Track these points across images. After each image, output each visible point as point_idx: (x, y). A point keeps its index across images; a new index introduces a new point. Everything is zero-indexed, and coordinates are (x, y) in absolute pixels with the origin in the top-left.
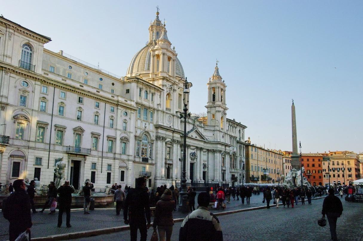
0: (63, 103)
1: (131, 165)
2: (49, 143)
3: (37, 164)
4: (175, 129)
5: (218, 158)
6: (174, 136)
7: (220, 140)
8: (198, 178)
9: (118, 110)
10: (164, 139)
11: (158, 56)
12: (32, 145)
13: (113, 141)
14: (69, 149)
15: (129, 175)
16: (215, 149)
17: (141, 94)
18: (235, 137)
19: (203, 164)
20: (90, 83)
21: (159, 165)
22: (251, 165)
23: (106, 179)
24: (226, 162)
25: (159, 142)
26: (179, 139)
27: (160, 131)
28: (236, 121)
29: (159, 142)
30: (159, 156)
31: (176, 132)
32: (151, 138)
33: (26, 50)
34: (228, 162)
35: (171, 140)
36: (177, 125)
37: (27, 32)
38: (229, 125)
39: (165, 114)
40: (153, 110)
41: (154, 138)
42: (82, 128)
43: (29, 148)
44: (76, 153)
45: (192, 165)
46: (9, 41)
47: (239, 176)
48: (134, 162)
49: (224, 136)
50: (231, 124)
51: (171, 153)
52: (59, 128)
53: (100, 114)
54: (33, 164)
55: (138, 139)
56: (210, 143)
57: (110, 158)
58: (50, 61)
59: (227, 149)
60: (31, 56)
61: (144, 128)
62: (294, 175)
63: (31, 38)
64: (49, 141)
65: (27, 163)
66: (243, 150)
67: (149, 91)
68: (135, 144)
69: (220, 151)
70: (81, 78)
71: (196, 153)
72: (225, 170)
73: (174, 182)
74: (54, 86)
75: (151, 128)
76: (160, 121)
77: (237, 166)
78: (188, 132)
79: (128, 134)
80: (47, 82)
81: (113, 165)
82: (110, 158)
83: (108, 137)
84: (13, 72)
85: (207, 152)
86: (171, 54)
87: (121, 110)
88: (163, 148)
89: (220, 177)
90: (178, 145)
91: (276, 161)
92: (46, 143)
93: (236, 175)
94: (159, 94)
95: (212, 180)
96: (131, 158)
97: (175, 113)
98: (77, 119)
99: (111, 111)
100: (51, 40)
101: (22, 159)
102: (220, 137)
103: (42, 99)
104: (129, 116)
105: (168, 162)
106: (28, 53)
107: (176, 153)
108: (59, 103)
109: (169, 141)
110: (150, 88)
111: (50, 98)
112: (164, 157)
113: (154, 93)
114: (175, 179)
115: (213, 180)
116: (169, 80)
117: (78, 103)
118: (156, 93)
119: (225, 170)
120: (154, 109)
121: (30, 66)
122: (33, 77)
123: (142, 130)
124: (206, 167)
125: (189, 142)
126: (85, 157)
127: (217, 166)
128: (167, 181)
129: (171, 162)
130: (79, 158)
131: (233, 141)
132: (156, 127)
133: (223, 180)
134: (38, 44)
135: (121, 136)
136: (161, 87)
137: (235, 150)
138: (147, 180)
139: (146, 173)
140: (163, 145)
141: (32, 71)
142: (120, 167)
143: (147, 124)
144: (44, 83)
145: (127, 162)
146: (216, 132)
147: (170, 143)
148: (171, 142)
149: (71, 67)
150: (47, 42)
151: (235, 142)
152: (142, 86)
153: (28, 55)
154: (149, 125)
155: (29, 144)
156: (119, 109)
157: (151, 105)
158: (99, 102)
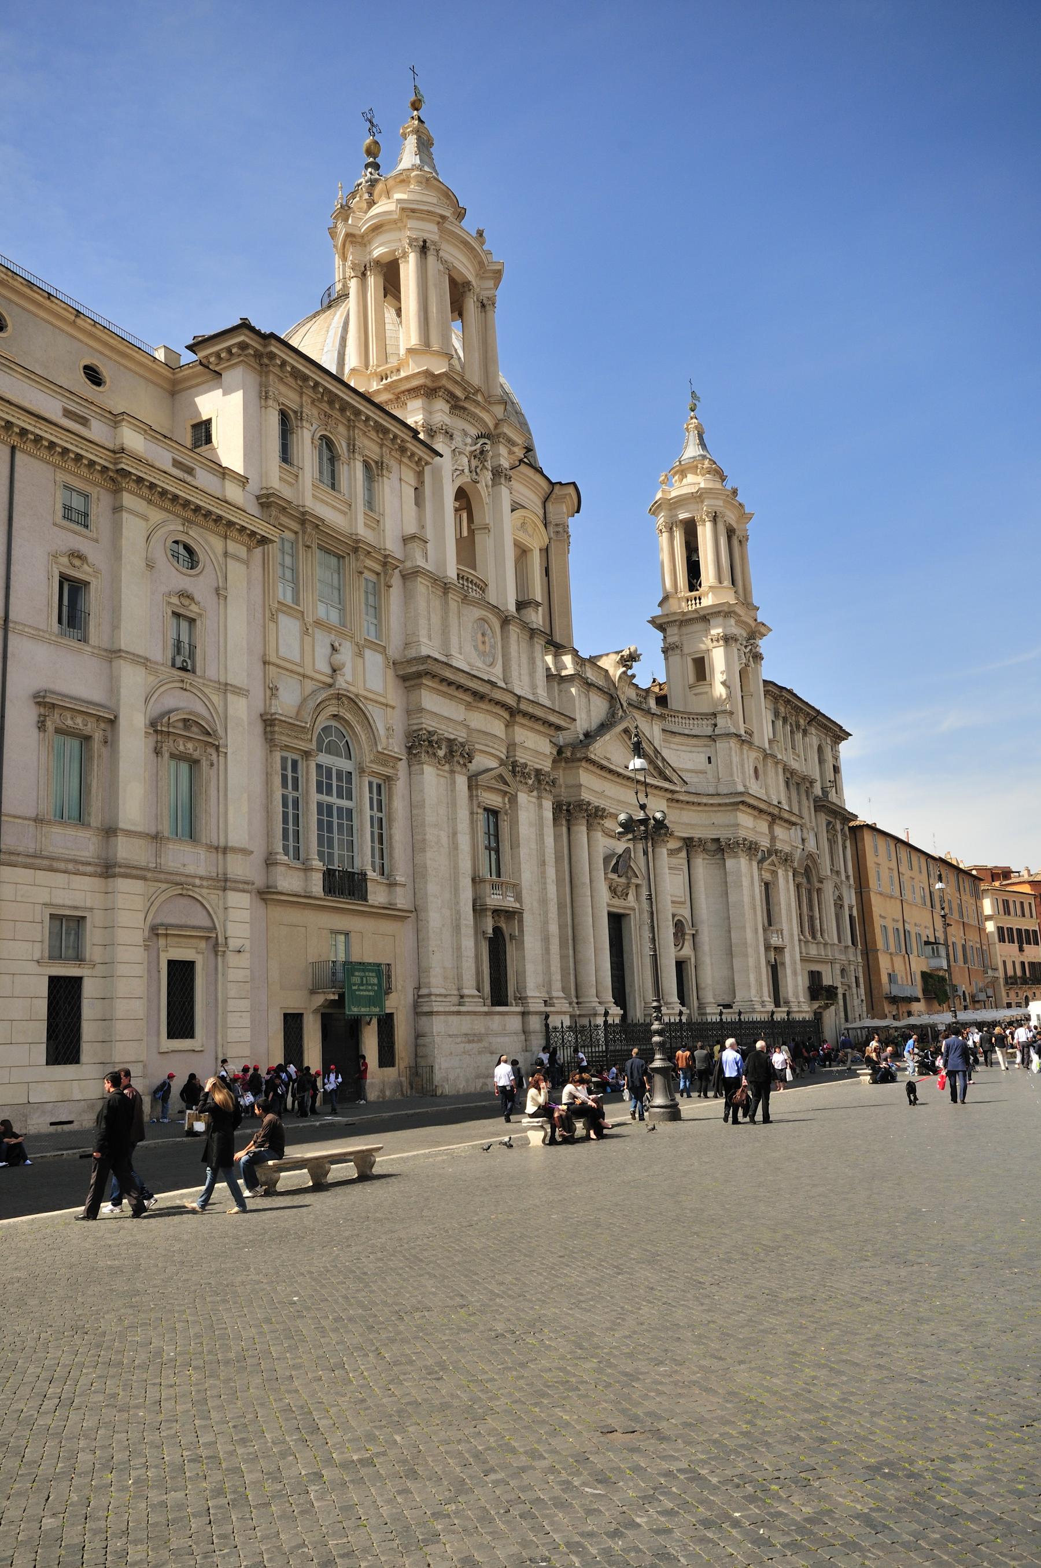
1: (246, 915)
5: (746, 882)
7: (745, 786)
9: (125, 515)
13: (87, 739)
15: (232, 993)
16: (723, 834)
18: (804, 778)
21: (436, 918)
22: (878, 923)
23: (40, 1030)
25: (425, 766)
26: (546, 765)
29: (425, 766)
30: (436, 860)
31: (525, 714)
32: (374, 740)
34: (789, 905)
35: (502, 763)
36: (526, 679)
38: (776, 714)
39: (453, 605)
40: (378, 568)
41: (396, 746)
47: (839, 978)
48: (266, 895)
49: (760, 772)
50: (782, 709)
55: (285, 740)
57: (74, 867)
59: (780, 837)
61: (329, 671)
66: (844, 848)
67: (344, 445)
68: (268, 776)
69: (750, 849)
72: (779, 950)
73: (535, 1023)
76: (430, 639)
78: (587, 735)
79: (215, 698)
82: (70, 867)
85: (684, 854)
86: (465, 261)
87: (146, 519)
88: (455, 812)
89: (760, 985)
90: (539, 798)
94: (410, 477)
96: (238, 868)
97: (512, 607)
102: (743, 773)
104: (209, 569)
105: (494, 900)
107: (533, 846)
110: (350, 426)
112: (466, 866)
113: (380, 465)
114: (543, 1008)
115: (728, 1006)
116: (466, 405)
118: (393, 463)
119: (779, 950)
120: (386, 562)
123: (310, 686)
124: (683, 934)
128: (497, 1017)
129: (509, 902)
132: (404, 678)
133: (777, 1004)
135: (155, 709)
138: (369, 1023)
140: (453, 790)
142: (155, 931)
145: (212, 898)
146: (721, 745)
147: (494, 784)
148: (501, 778)
151: (809, 807)
152: (294, 396)
154: (360, 654)
156: (131, 512)
157: (362, 531)
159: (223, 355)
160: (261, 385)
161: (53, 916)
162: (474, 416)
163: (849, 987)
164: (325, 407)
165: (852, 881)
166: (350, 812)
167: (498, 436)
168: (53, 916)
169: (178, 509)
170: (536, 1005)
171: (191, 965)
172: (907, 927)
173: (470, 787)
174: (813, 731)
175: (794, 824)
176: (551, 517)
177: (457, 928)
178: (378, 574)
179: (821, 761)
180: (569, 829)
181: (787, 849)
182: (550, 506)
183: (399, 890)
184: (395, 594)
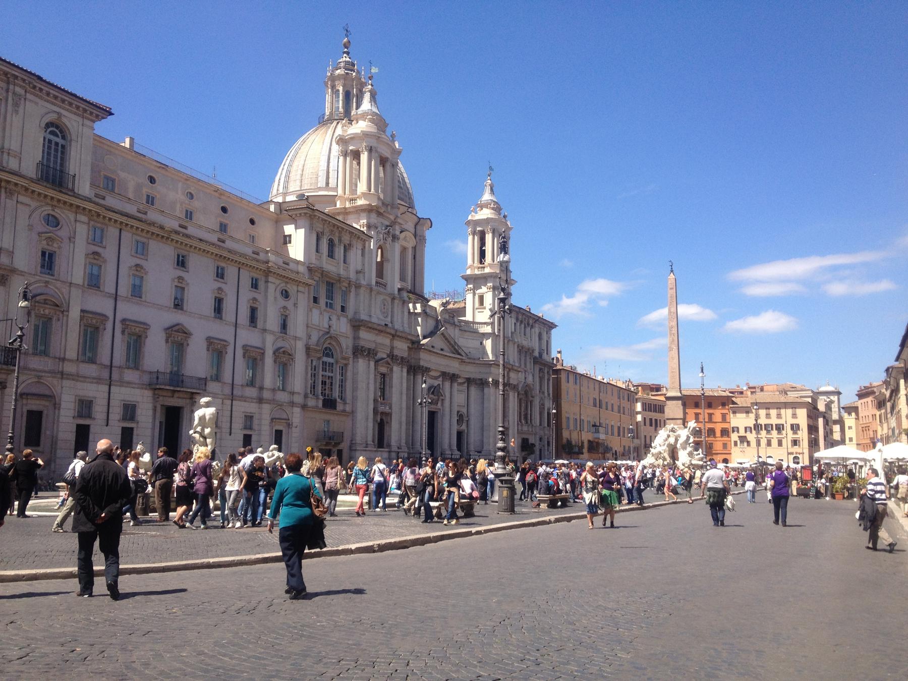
0: (141, 267)
1: (298, 415)
2: (109, 364)
3: (80, 416)
4: (396, 331)
6: (394, 346)
8: (446, 446)
10: (370, 353)
11: (356, 155)
12: (69, 368)
13: (256, 359)
14: (158, 378)
17: (320, 247)
19: (458, 412)
20: (200, 218)
21: (360, 416)
24: (509, 408)
26: (405, 355)
27: (364, 334)
28: (531, 312)
30: (361, 394)
31: (398, 336)
32: (342, 352)
33: (52, 137)
34: (514, 410)
35: (388, 356)
37: (57, 94)
38: (517, 319)
41: (349, 353)
42: (186, 328)
43: (63, 375)
44: (172, 388)
45: (432, 415)
46: (14, 115)
48: (304, 407)
51: (387, 388)
52: (133, 328)
53: (226, 295)
54: (73, 415)
56: (474, 363)
58: (104, 163)
60: (63, 153)
61: (328, 327)
62: (672, 440)
63: (64, 108)
64: (109, 359)
65: (59, 413)
70: (178, 206)
71: (441, 387)
74: (118, 226)
75: (342, 327)
77: (533, 418)
80: (104, 217)
81: (256, 417)
83: (245, 348)
84: (24, 192)
85: (466, 385)
90: (402, 368)
91: (621, 407)
92: (101, 364)
93: (532, 441)
94: (360, 247)
95: (479, 452)
97: (396, 292)
98: (172, 306)
99: (252, 287)
100: (113, 114)
101: (47, 403)
103: (92, 256)
105: (381, 409)
106: (57, 144)
108: (130, 268)
109: (383, 359)
111: (109, 253)
112: (372, 396)
115: (480, 452)
117: (176, 269)
121: (61, 178)
122: (71, 205)
123: (321, 333)
124: (463, 420)
125: (425, 359)
126: (191, 398)
127: (489, 418)
129: (387, 409)
130: (180, 400)
131: (525, 360)
132: (354, 326)
134: (81, 123)
135: (275, 347)
136: (365, 229)
137: (530, 379)
138: (334, 452)
139: (330, 434)
141: (69, 190)
143: (334, 318)
144: (95, 218)
149: (152, 180)
150: (103, 118)
151: (530, 362)
153: (56, 150)
154: (339, 319)
155: (63, 368)
157: (342, 272)
158: (223, 264)
159: (298, 215)
160: (310, 224)
161: (245, 416)
162: (388, 218)
163: (544, 446)
164: (332, 228)
165: (551, 395)
166: (332, 377)
167: (396, 222)
168: (245, 416)
169: (284, 279)
170: (394, 449)
171: (281, 431)
172: (582, 418)
173: (375, 366)
174: (537, 325)
175: (519, 371)
176: (418, 232)
177: (367, 419)
178: (346, 288)
179: (540, 338)
180: (414, 376)
181: (515, 383)
182: (418, 227)
183: (347, 405)
184: (352, 295)
